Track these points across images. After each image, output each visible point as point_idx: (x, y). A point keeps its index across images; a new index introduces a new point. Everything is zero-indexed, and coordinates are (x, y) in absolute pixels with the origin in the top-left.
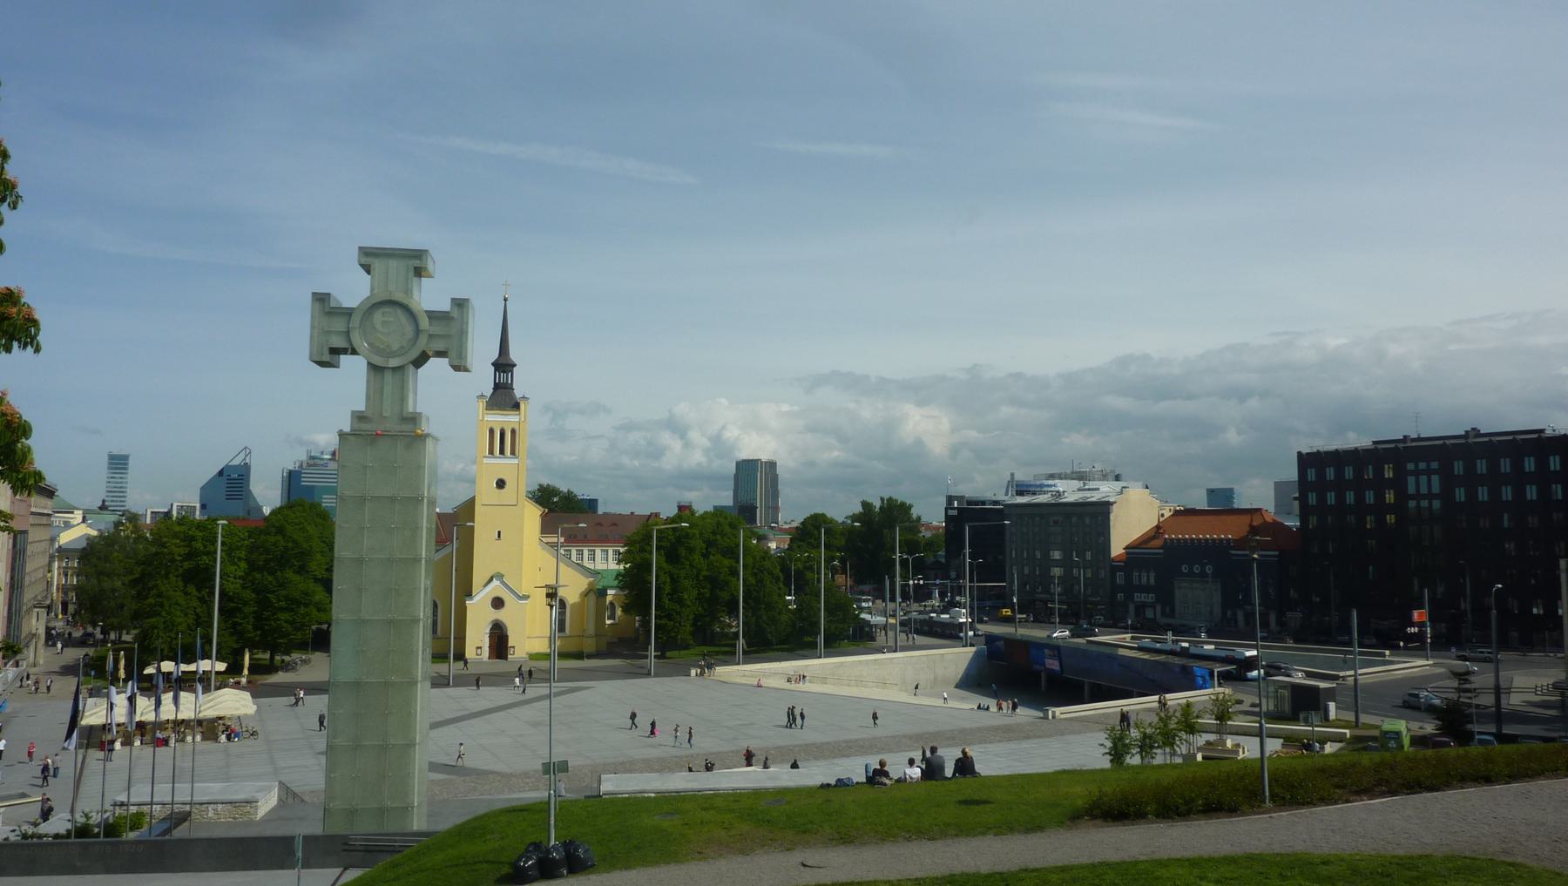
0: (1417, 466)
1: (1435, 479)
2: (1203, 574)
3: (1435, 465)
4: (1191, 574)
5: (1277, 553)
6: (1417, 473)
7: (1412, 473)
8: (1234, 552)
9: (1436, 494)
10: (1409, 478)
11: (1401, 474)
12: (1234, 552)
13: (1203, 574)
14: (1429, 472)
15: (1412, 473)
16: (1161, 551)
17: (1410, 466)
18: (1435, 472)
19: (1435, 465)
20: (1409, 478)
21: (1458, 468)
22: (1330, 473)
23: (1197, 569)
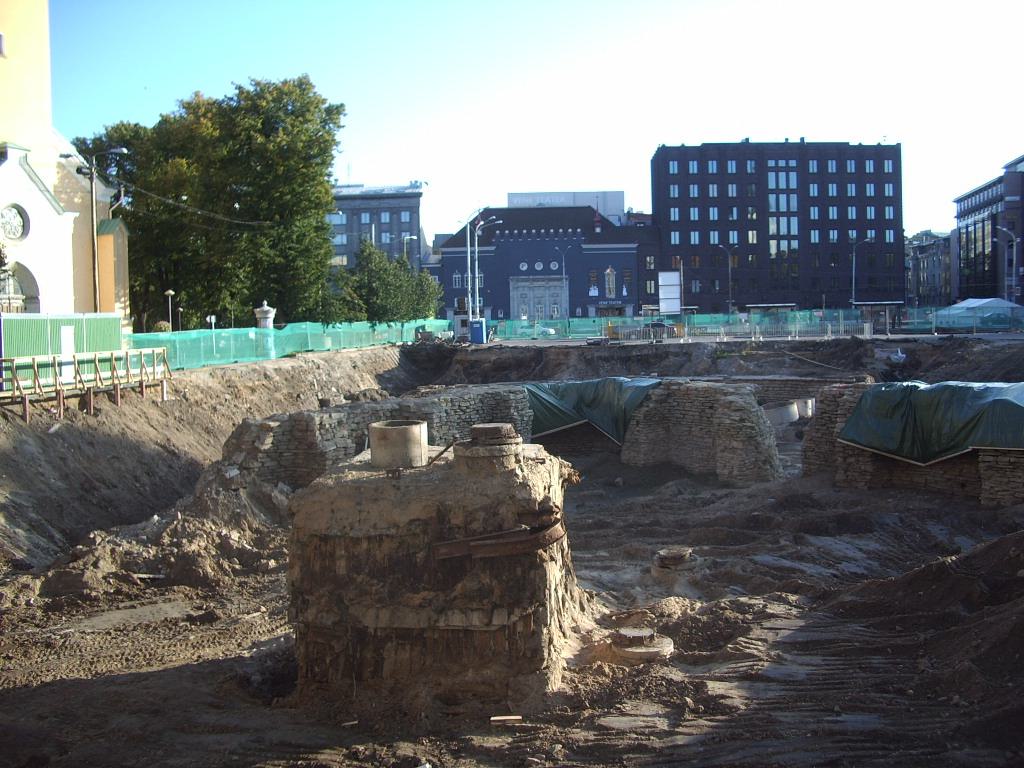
0: (777, 163)
1: (793, 176)
2: (547, 271)
3: (793, 163)
4: (531, 271)
5: (635, 246)
6: (777, 170)
7: (772, 169)
8: (584, 246)
9: (772, 190)
10: (769, 174)
11: (762, 170)
12: (584, 246)
13: (547, 271)
14: (787, 170)
15: (772, 169)
16: (493, 248)
17: (771, 163)
18: (792, 169)
19: (793, 163)
20: (769, 174)
21: (813, 167)
22: (693, 167)
23: (539, 266)
